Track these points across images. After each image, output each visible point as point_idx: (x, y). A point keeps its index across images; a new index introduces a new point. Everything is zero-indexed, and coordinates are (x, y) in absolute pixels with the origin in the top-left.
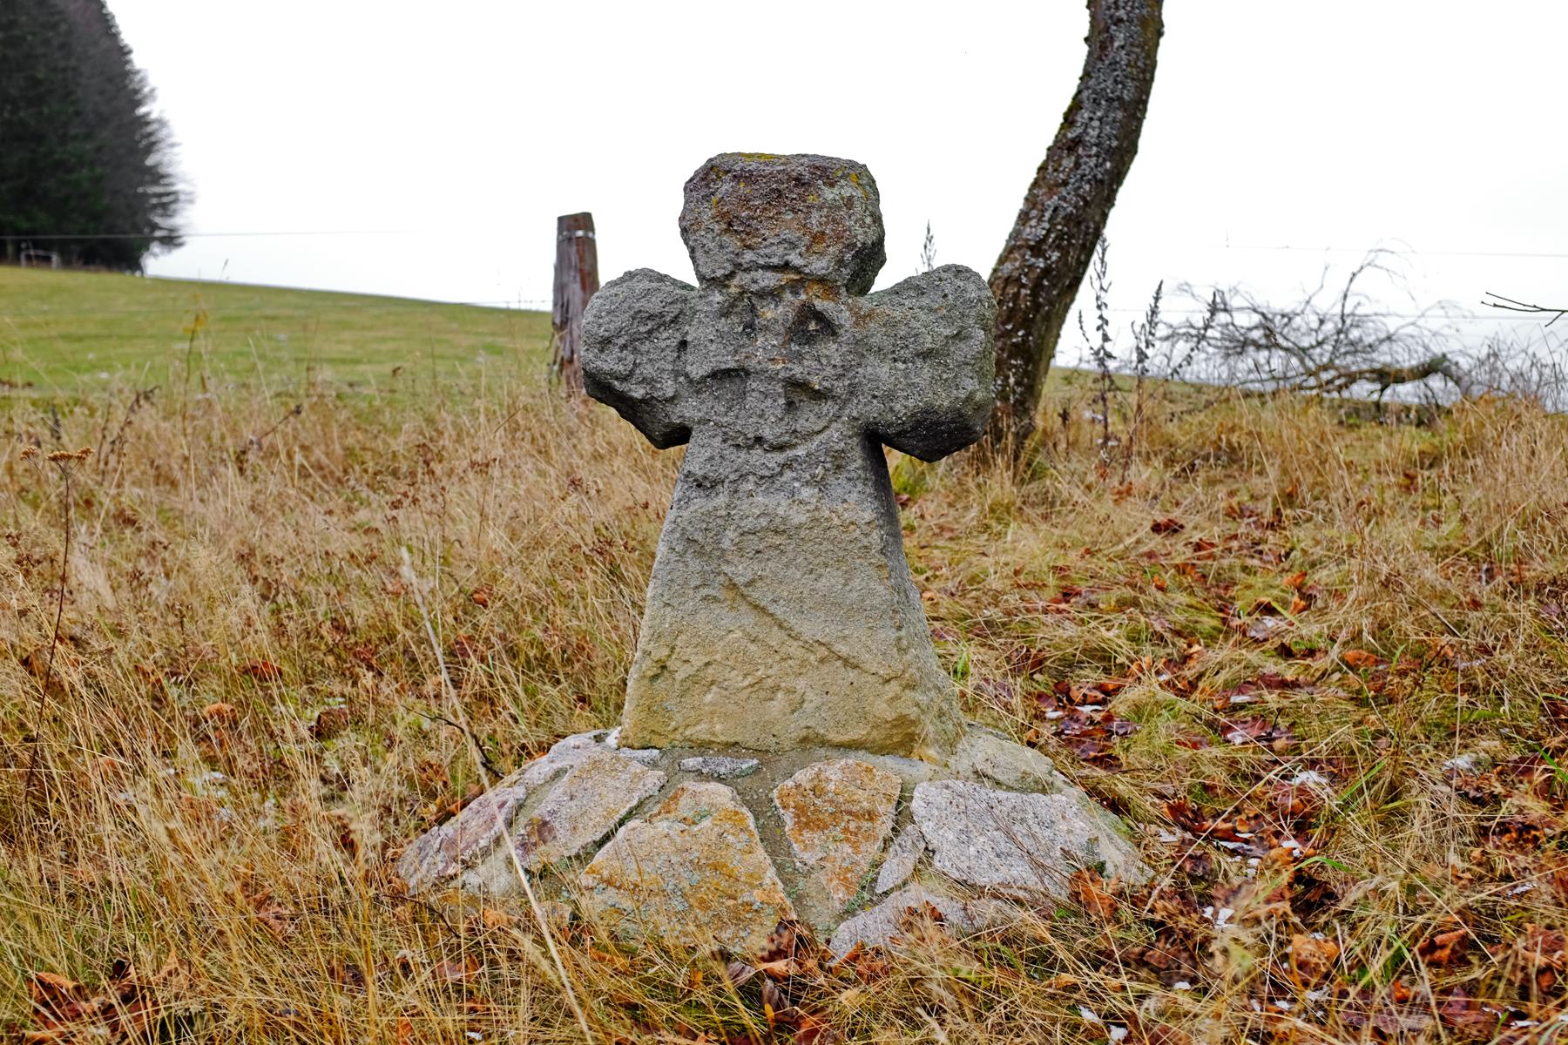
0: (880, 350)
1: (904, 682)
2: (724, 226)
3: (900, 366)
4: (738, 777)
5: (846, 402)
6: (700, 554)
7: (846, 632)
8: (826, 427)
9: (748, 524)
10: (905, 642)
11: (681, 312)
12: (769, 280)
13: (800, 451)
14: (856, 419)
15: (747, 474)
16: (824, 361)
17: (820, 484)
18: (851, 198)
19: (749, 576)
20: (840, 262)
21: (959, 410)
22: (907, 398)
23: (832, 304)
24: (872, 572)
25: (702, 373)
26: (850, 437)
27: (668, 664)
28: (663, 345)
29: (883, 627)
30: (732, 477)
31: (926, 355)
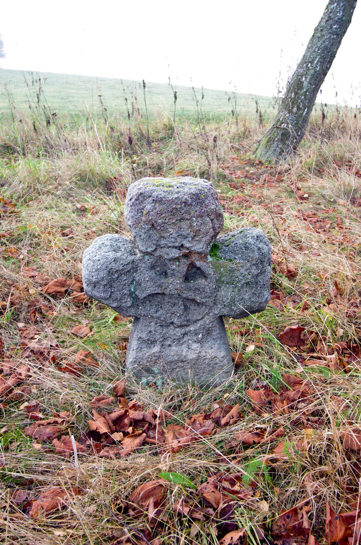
8: (203, 318)
9: (170, 359)
25: (144, 295)
28: (123, 283)
30: (161, 339)
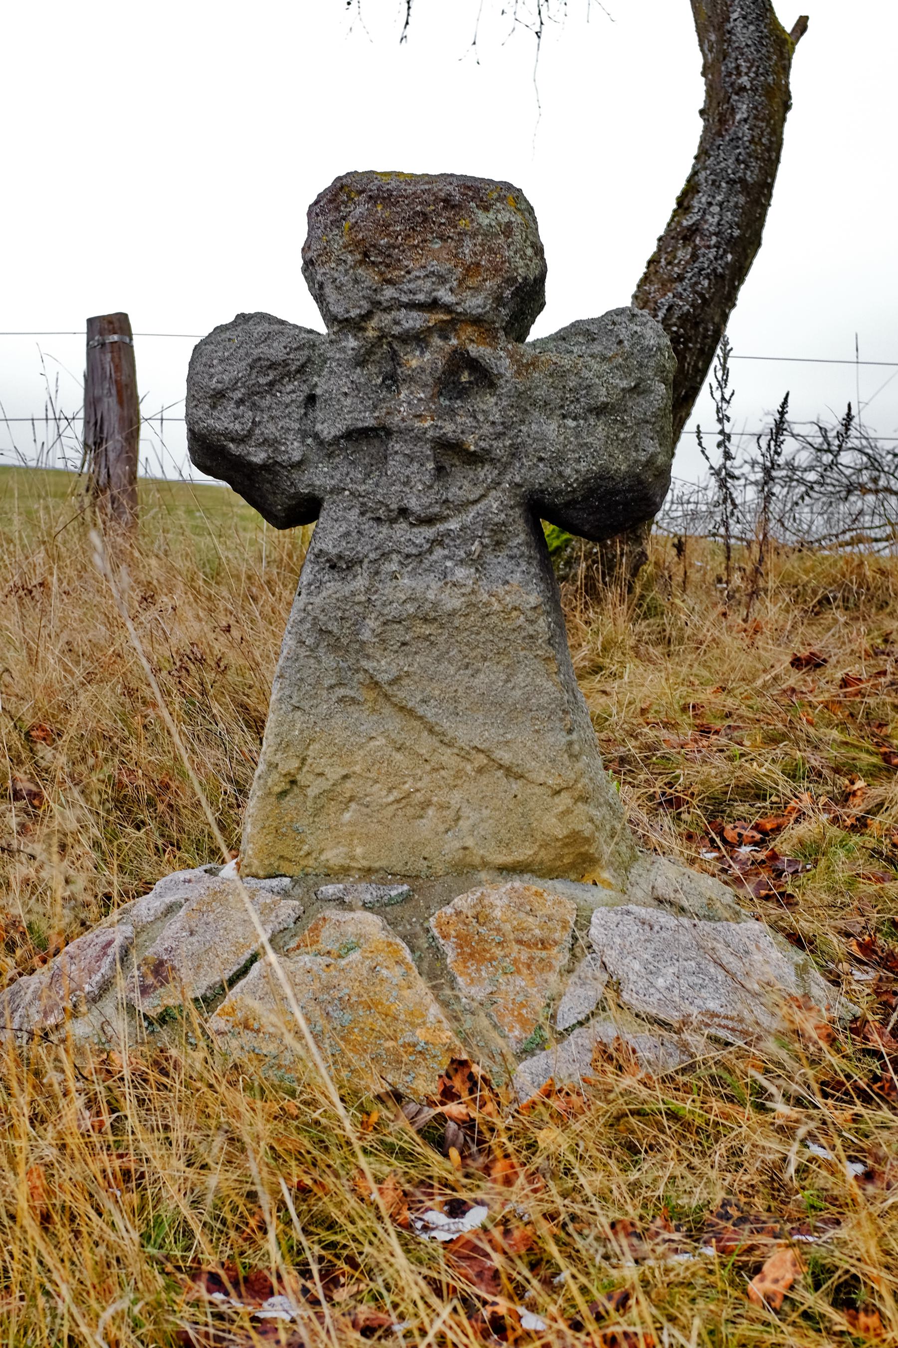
0: (546, 404)
1: (576, 794)
2: (359, 257)
3: (570, 423)
4: (386, 905)
5: (506, 466)
6: (335, 647)
7: (509, 736)
8: (483, 496)
9: (392, 611)
10: (576, 747)
11: (309, 360)
12: (414, 321)
13: (453, 525)
14: (519, 486)
15: (391, 552)
16: (481, 418)
17: (477, 562)
18: (509, 224)
19: (394, 672)
20: (499, 300)
21: (638, 476)
22: (578, 461)
23: (489, 350)
24: (539, 665)
25: (334, 432)
26: (512, 508)
27: (299, 777)
28: (287, 399)
29: (552, 729)
30: (372, 556)
31: (600, 411)
